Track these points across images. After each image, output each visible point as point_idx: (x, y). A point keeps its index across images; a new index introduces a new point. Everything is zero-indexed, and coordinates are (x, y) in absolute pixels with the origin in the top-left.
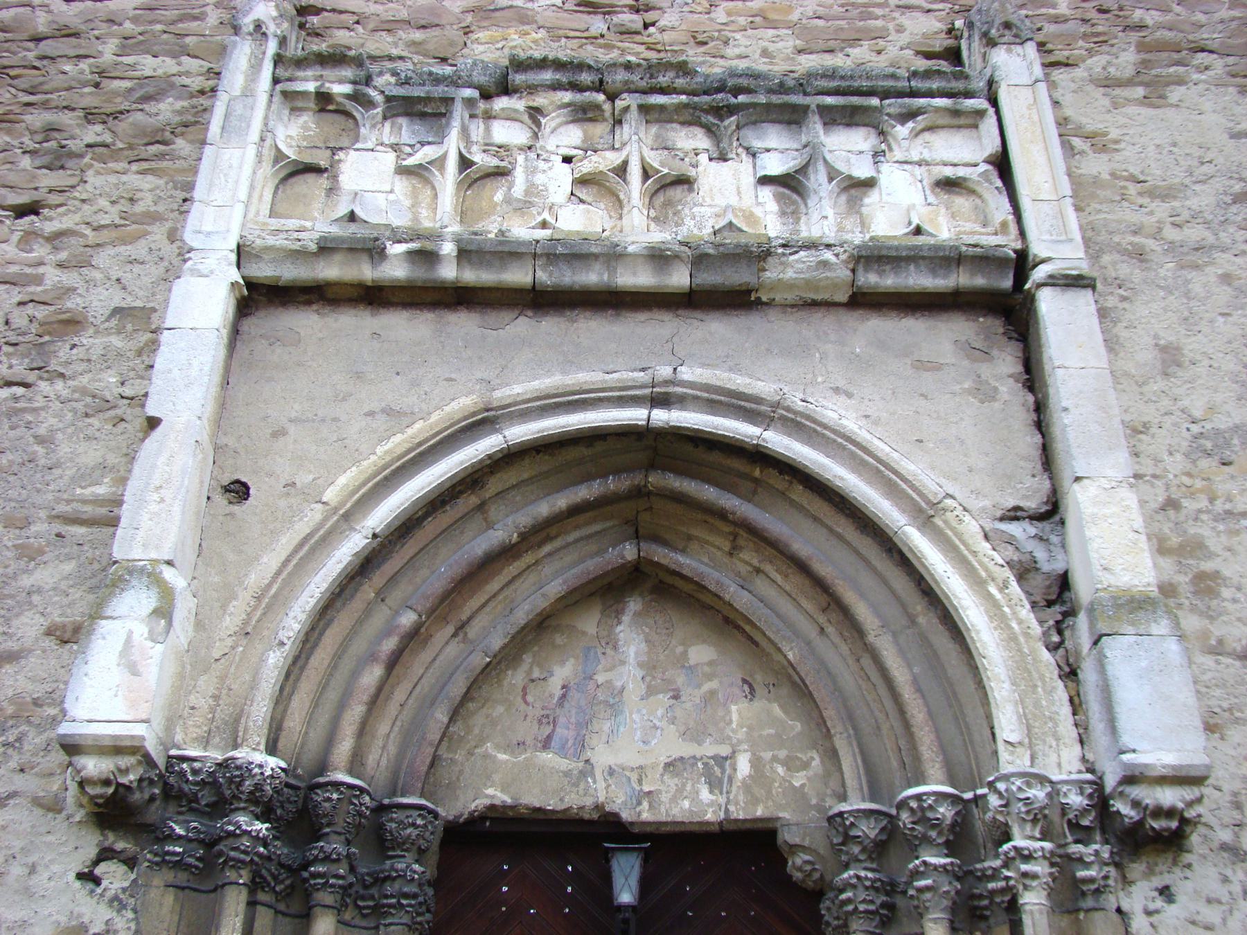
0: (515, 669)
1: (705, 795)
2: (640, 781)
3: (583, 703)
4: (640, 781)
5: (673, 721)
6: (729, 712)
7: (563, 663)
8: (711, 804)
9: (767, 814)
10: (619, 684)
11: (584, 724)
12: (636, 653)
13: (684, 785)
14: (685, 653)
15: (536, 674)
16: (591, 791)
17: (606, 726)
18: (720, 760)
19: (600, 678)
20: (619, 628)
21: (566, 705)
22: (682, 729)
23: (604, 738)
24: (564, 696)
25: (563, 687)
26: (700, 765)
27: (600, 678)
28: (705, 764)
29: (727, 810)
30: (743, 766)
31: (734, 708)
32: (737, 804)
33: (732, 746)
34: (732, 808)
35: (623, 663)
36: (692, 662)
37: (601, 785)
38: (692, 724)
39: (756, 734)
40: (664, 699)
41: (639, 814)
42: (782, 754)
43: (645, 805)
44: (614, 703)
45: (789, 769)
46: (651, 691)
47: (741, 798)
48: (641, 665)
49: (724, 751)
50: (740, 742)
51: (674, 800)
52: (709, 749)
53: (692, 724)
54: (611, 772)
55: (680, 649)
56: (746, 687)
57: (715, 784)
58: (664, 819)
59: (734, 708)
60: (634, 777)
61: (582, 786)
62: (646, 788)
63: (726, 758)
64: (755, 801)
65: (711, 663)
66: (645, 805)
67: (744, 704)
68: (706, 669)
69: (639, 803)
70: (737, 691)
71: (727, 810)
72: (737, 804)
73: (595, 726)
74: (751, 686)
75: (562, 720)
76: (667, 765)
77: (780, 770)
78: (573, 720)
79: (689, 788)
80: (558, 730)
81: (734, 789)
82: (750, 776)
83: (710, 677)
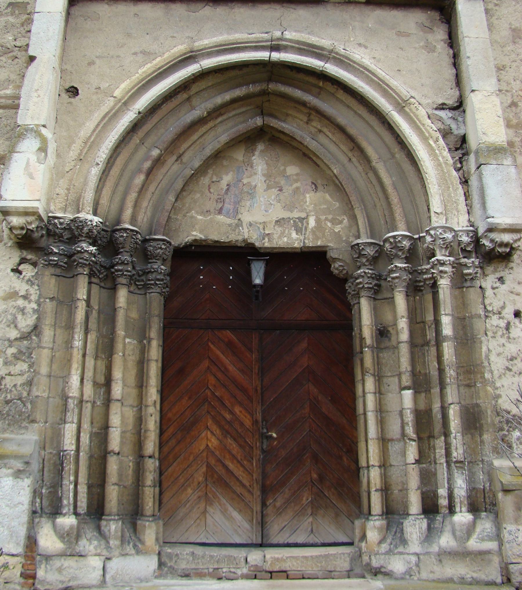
0: (205, 176)
1: (294, 235)
2: (264, 229)
3: (237, 192)
4: (264, 229)
5: (279, 201)
6: (306, 197)
7: (227, 174)
8: (296, 240)
9: (323, 244)
10: (254, 184)
11: (237, 203)
12: (262, 170)
13: (284, 231)
14: (285, 169)
15: (214, 179)
16: (241, 233)
17: (248, 203)
18: (301, 219)
19: (245, 181)
20: (254, 158)
21: (229, 193)
22: (284, 205)
23: (247, 209)
24: (228, 189)
25: (227, 185)
26: (292, 221)
27: (245, 181)
28: (294, 221)
29: (304, 242)
30: (312, 222)
31: (308, 195)
32: (309, 239)
33: (307, 213)
34: (306, 241)
35: (255, 174)
36: (288, 174)
37: (246, 230)
38: (288, 203)
39: (318, 208)
40: (275, 191)
41: (264, 243)
42: (330, 217)
43: (266, 239)
44: (252, 193)
45: (333, 224)
46: (269, 187)
47: (311, 237)
48: (264, 175)
49: (303, 215)
50: (310, 211)
51: (280, 237)
52: (296, 214)
53: (288, 203)
54: (251, 224)
55: (282, 168)
56: (313, 186)
57: (298, 231)
58: (275, 246)
59: (308, 195)
60: (261, 227)
61: (237, 231)
62: (267, 232)
63: (304, 219)
64: (317, 238)
65: (297, 175)
66: (266, 239)
67: (312, 194)
68: (295, 177)
69: (264, 239)
70: (309, 187)
71: (304, 242)
72: (309, 239)
73: (243, 203)
74: (315, 185)
75: (227, 200)
76: (277, 222)
77: (329, 224)
78: (232, 200)
79: (287, 232)
80: (226, 205)
81: (308, 232)
82: (315, 227)
83: (296, 181)
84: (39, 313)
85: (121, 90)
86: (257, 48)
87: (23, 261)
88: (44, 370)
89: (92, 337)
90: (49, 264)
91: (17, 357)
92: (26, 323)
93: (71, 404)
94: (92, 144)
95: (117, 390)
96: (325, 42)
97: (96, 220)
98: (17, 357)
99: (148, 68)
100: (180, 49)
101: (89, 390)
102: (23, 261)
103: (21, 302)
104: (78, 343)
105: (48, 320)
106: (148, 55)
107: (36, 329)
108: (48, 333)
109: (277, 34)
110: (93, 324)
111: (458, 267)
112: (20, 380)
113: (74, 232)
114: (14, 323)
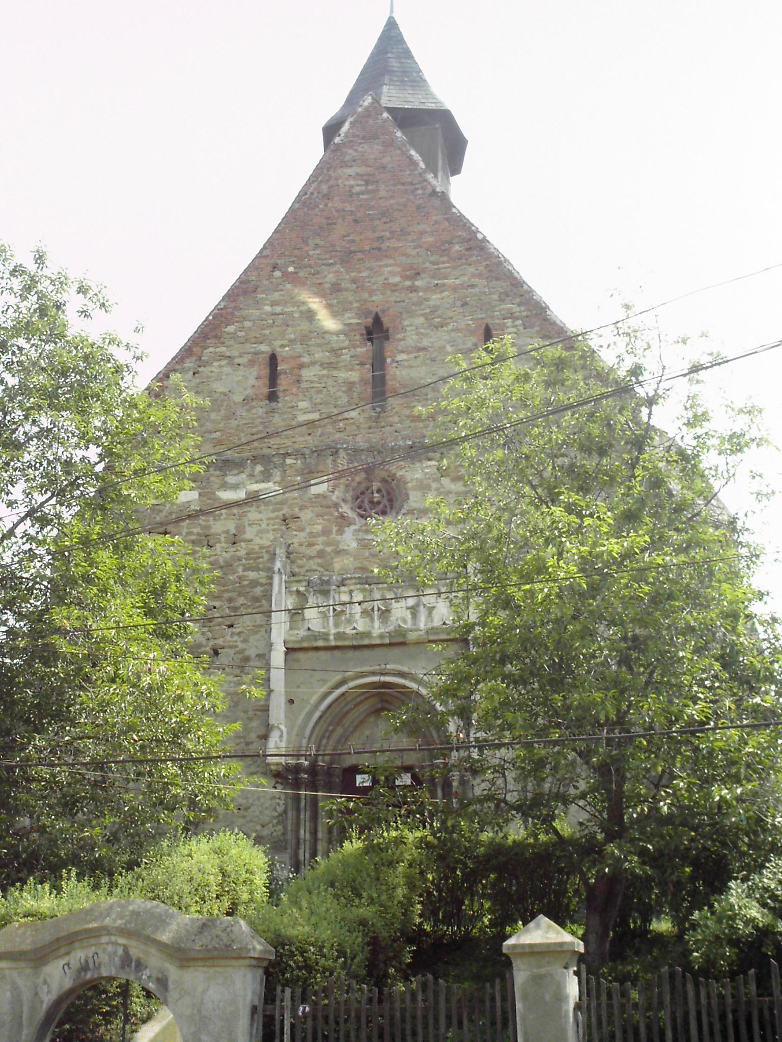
84: (286, 805)
85: (314, 699)
86: (374, 674)
87: (277, 782)
88: (289, 828)
89: (308, 813)
90: (288, 783)
91: (278, 823)
92: (280, 809)
93: (301, 841)
94: (303, 727)
95: (320, 835)
96: (405, 669)
97: (307, 763)
98: (278, 823)
99: (324, 689)
100: (338, 677)
101: (308, 836)
102: (277, 782)
103: (278, 801)
104: (302, 817)
105: (290, 807)
106: (324, 681)
107: (285, 812)
108: (290, 813)
109: (383, 666)
110: (308, 808)
111: (462, 777)
112: (279, 833)
113: (297, 769)
114: (275, 810)
